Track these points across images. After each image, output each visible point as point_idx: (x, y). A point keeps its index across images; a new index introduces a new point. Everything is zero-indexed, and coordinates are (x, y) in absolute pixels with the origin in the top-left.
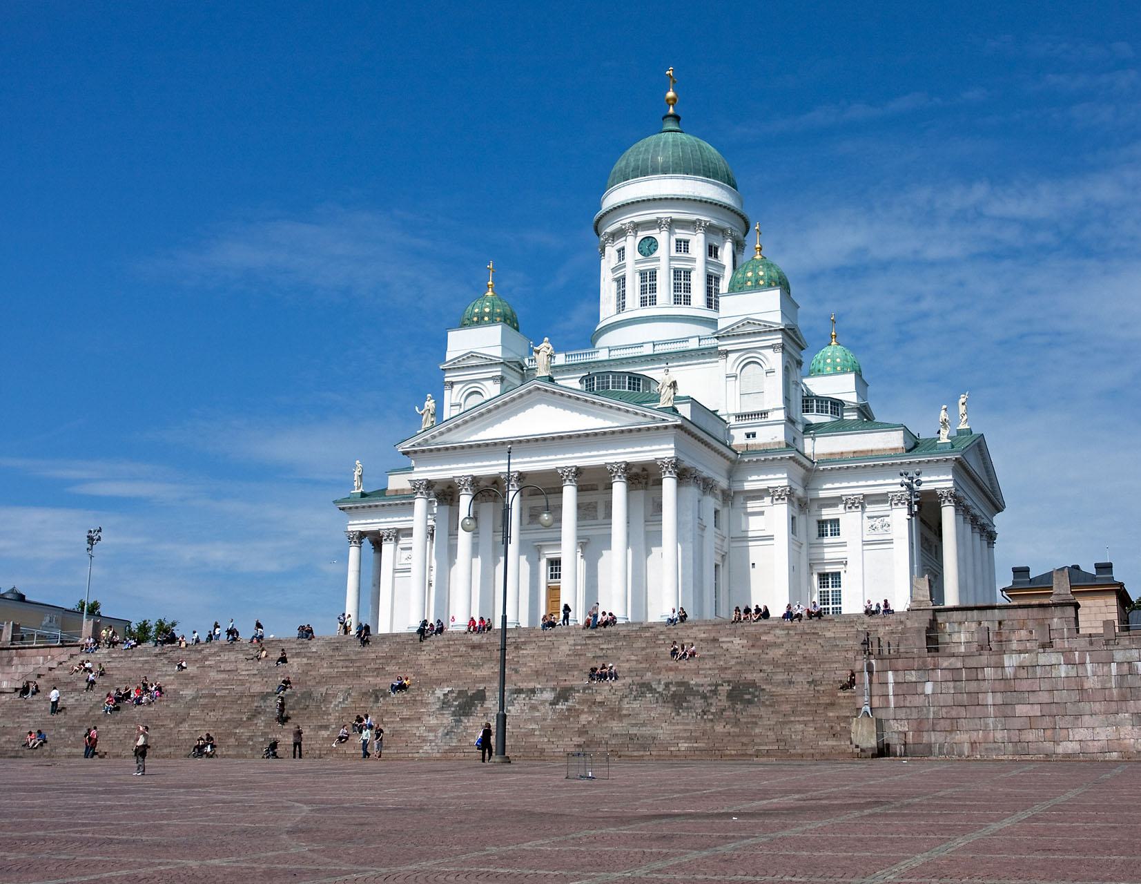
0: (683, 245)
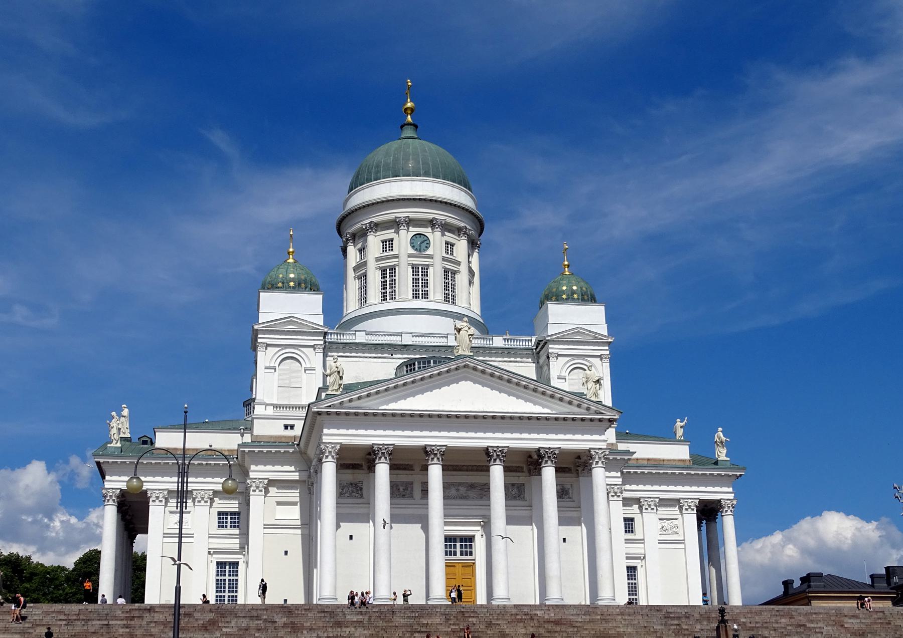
0: (449, 246)
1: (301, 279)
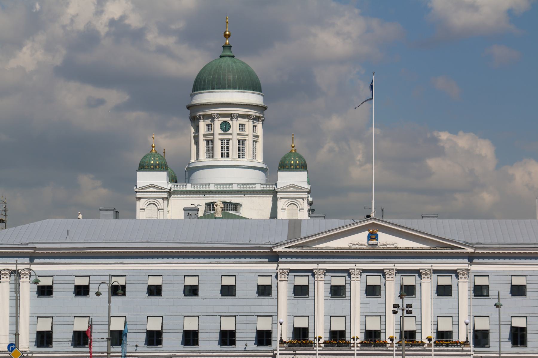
0: (242, 127)
1: (157, 163)
